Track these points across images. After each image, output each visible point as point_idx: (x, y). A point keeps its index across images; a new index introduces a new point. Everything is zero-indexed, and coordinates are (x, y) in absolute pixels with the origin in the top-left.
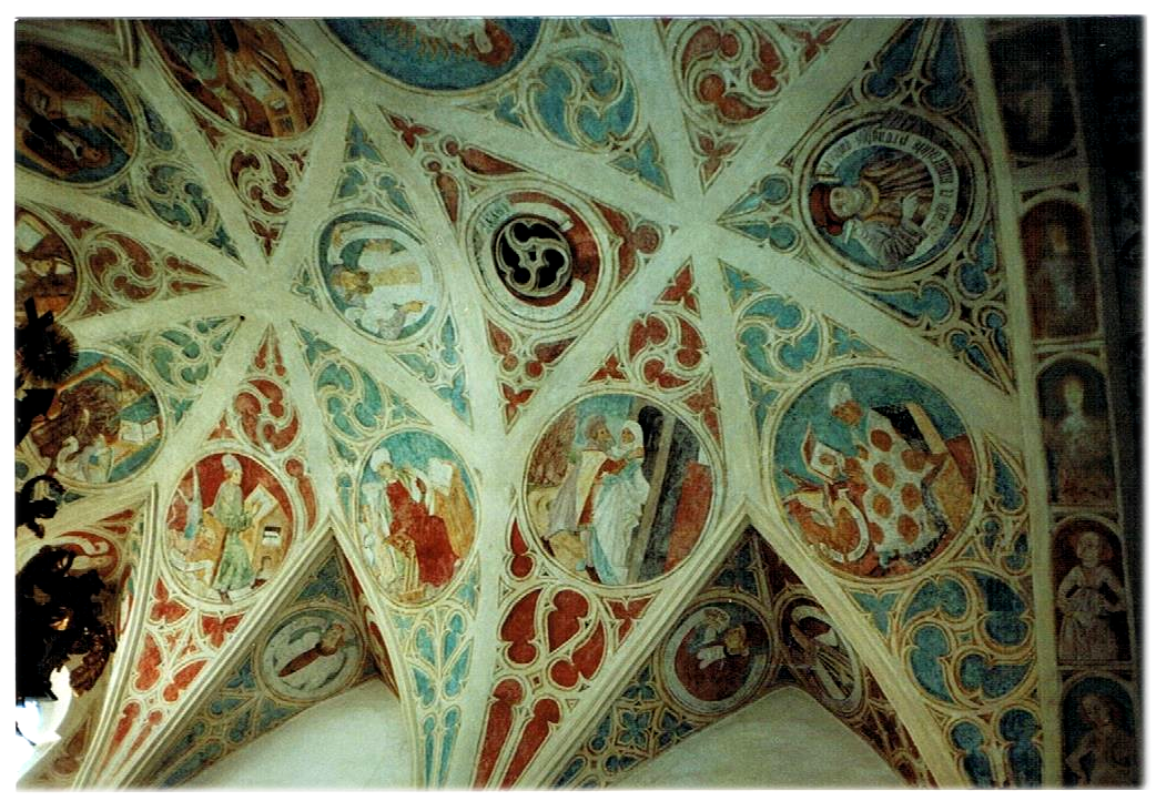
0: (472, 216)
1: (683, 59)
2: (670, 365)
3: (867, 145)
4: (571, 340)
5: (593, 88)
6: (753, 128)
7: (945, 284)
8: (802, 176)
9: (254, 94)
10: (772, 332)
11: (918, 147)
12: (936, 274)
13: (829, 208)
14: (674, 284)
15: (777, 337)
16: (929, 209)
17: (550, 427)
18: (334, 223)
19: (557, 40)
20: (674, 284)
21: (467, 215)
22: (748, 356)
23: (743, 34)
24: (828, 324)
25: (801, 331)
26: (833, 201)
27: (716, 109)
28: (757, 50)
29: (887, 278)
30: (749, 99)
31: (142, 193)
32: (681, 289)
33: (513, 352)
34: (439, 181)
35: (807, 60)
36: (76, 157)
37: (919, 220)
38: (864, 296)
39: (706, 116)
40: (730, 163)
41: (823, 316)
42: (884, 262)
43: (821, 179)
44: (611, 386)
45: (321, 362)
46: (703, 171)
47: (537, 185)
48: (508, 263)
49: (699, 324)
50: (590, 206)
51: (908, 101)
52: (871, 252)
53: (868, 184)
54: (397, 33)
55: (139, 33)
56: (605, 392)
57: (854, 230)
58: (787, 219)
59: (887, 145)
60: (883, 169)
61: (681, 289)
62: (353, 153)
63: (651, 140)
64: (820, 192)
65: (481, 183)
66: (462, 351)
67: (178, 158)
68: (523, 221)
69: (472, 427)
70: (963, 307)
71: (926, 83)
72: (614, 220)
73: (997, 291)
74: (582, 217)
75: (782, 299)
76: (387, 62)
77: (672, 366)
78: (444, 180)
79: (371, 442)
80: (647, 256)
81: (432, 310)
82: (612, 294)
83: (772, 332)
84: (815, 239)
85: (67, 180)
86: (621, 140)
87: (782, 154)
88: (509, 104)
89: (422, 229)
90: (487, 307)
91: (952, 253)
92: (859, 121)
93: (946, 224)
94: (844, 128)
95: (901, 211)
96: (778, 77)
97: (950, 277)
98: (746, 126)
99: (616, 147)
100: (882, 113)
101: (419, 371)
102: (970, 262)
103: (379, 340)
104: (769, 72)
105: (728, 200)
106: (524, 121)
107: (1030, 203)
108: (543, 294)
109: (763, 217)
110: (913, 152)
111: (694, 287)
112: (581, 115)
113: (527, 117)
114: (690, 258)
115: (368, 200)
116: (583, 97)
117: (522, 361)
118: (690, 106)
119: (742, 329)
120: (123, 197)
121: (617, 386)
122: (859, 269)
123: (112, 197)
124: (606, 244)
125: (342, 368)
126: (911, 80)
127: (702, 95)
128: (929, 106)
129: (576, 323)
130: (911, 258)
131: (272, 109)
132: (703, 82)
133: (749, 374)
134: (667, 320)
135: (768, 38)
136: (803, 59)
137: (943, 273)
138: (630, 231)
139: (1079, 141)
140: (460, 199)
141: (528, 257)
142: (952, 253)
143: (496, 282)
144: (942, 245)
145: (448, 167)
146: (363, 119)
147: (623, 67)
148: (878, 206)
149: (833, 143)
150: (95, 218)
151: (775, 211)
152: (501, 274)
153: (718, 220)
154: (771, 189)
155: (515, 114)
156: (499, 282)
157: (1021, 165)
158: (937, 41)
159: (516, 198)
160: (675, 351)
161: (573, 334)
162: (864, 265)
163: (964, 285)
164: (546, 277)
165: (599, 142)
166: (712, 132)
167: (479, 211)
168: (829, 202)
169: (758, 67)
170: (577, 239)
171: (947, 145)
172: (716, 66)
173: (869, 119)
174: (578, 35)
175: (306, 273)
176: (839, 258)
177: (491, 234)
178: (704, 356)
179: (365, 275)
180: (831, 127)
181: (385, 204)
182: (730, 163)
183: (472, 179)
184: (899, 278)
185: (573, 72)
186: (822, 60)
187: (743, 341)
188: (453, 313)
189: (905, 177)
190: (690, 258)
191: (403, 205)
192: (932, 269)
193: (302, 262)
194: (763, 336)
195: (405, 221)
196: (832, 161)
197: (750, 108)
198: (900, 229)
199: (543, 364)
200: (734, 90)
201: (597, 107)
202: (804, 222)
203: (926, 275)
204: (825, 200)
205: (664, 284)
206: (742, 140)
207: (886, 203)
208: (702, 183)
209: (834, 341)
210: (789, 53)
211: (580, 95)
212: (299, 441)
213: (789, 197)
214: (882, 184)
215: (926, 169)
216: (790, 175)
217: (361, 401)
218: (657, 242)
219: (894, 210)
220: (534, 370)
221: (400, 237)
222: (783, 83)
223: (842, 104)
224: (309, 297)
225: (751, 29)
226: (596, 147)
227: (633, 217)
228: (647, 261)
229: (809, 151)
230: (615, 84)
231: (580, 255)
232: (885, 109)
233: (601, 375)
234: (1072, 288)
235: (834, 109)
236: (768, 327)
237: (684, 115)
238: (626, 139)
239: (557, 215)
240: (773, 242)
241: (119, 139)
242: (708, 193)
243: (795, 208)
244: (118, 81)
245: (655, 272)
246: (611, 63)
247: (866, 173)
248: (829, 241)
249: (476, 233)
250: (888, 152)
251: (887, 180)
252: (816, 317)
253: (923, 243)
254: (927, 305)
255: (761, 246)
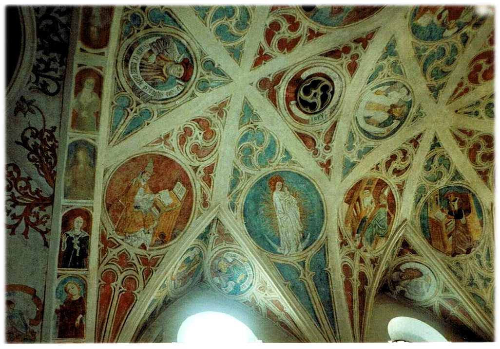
0: (328, 121)
1: (213, 150)
2: (286, 26)
3: (160, 91)
4: (321, 55)
5: (251, 151)
6: (201, 114)
7: (148, 22)
8: (190, 88)
9: (372, 198)
10: (232, 26)
11: (141, 83)
12: (151, 28)
13: (185, 71)
14: (263, 62)
15: (231, 22)
16: (145, 55)
17: (358, 21)
18: (384, 138)
19: (254, 175)
20: (263, 62)
21: (329, 123)
22: (249, 17)
23: (188, 152)
24: (206, 22)
25: (219, 22)
26: (182, 72)
27: (211, 126)
28: (186, 143)
29: (172, 33)
30: (197, 126)
31: (448, 175)
32: (262, 58)
33: (350, 61)
34: (330, 141)
35: (169, 134)
36: (458, 199)
37: (151, 52)
38: (185, 29)
39: (216, 125)
40: (216, 103)
41: (206, 26)
42: (171, 40)
43: (183, 84)
44: (318, 27)
45: (410, 149)
46: (227, 104)
47: (294, 124)
48: (327, 95)
49: (262, 39)
50: (279, 106)
51: (138, 104)
52: (175, 46)
53: (166, 75)
54: (304, 204)
55: (394, 232)
56: (322, 26)
57: (178, 58)
58: (204, 73)
59: (152, 88)
60: (158, 79)
61: (262, 58)
62: (354, 165)
63: (241, 123)
64: (186, 78)
65: (315, 134)
66: (373, 69)
67: (422, 182)
68: (309, 111)
69: (393, 36)
70: (144, 11)
71: (129, 109)
72: (273, 98)
73: (126, 13)
74: (285, 103)
75: (221, 39)
76: (315, 196)
77: (285, 25)
78: (328, 141)
79: (448, 40)
80: (268, 77)
81: (372, 89)
82: (292, 67)
83: (232, 26)
84: (196, 60)
85: (470, 191)
86: (252, 128)
87: (194, 100)
88: (284, 160)
89: (351, 124)
90: (348, 81)
91: (141, 34)
92: (160, 102)
93: (140, 46)
94: (166, 101)
95: (157, 58)
96: (182, 131)
97: (145, 25)
98: (203, 116)
99: (255, 126)
100: (150, 102)
101: (399, 66)
102: (135, 28)
103: (406, 84)
104: (185, 134)
105: (223, 89)
106: (283, 151)
107: (102, 50)
108: (320, 78)
109: (213, 76)
110: (143, 81)
111: (256, 57)
112: (261, 144)
113: (281, 152)
114: (251, 70)
115: (363, 142)
116: (257, 150)
117: (349, 56)
118: (220, 131)
119: (245, 31)
120: (457, 175)
121: (315, 27)
122: (183, 41)
123: (461, 178)
124: (282, 89)
125: (432, 77)
126: (134, 113)
127: (213, 133)
128: (131, 99)
129: (316, 61)
130: (160, 38)
131: (370, 191)
132: (210, 138)
133: (252, 9)
134: (276, 47)
135: (180, 147)
136: (170, 135)
137: (148, 27)
138: (270, 90)
139: (76, 70)
140: (327, 130)
141: (317, 95)
142: (141, 34)
143: (337, 90)
144: (145, 38)
145: (322, 145)
146: (339, 178)
147: (237, 154)
148: (165, 64)
149: (172, 97)
150: (475, 173)
151: (207, 77)
152: (333, 93)
153: (232, 82)
154: (204, 87)
155: (285, 155)
156: (335, 90)
157: (101, 68)
158: (119, 126)
159: (306, 122)
160: (279, 32)
161: (320, 57)
162: (180, 42)
163: (140, 20)
164: (315, 84)
165: (261, 131)
166: (216, 118)
167: (324, 122)
168: (184, 73)
169: (188, 137)
170: (292, 95)
171: (129, 79)
172: (203, 142)
173: (156, 102)
174: (246, 172)
175: (413, 121)
176: (190, 49)
177: (325, 111)
178: (268, 24)
179: (389, 112)
180: (171, 104)
181: (358, 139)
182: (216, 103)
183: (317, 136)
184: (168, 32)
185: (255, 160)
186: (164, 133)
187: (247, 25)
188: (365, 84)
189: (150, 72)
190: (251, 70)
191: (351, 136)
192: (153, 30)
193: (410, 126)
194: (237, 25)
195: (355, 128)
196: (176, 90)
197: (198, 123)
198: (159, 50)
199: (341, 50)
200: (201, 132)
201: (254, 144)
202: (197, 68)
203: (155, 29)
204: (185, 74)
205: (268, 63)
206: (163, 256)
207: (162, 64)
208: (230, 99)
209: (207, 13)
210: (175, 139)
211: (258, 151)
212: (480, 51)
213: (199, 81)
214: (160, 73)
215: (141, 72)
216: (195, 91)
217: (436, 60)
218: (261, 81)
219: (159, 60)
220: (347, 49)
221: (363, 124)
222: (182, 128)
223: (163, 112)
224: (421, 111)
225: (184, 152)
226: (263, 129)
227: (265, 96)
228: (270, 75)
229: (183, 97)
230: (243, 150)
231: (295, 88)
232: (148, 104)
233: (319, 34)
234: (93, 13)
235: (167, 111)
236: (233, 28)
237: (223, 128)
238: (250, 128)
239: (294, 109)
240: (214, 65)
241: (437, 198)
242: (229, 95)
243: (198, 75)
244: (417, 217)
245: (268, 69)
246: (240, 158)
247: (164, 79)
248: (191, 57)
249: (331, 113)
250: (153, 85)
251: (158, 73)
252: (210, 26)
253: (152, 42)
254: (159, 17)
255: (219, 65)
